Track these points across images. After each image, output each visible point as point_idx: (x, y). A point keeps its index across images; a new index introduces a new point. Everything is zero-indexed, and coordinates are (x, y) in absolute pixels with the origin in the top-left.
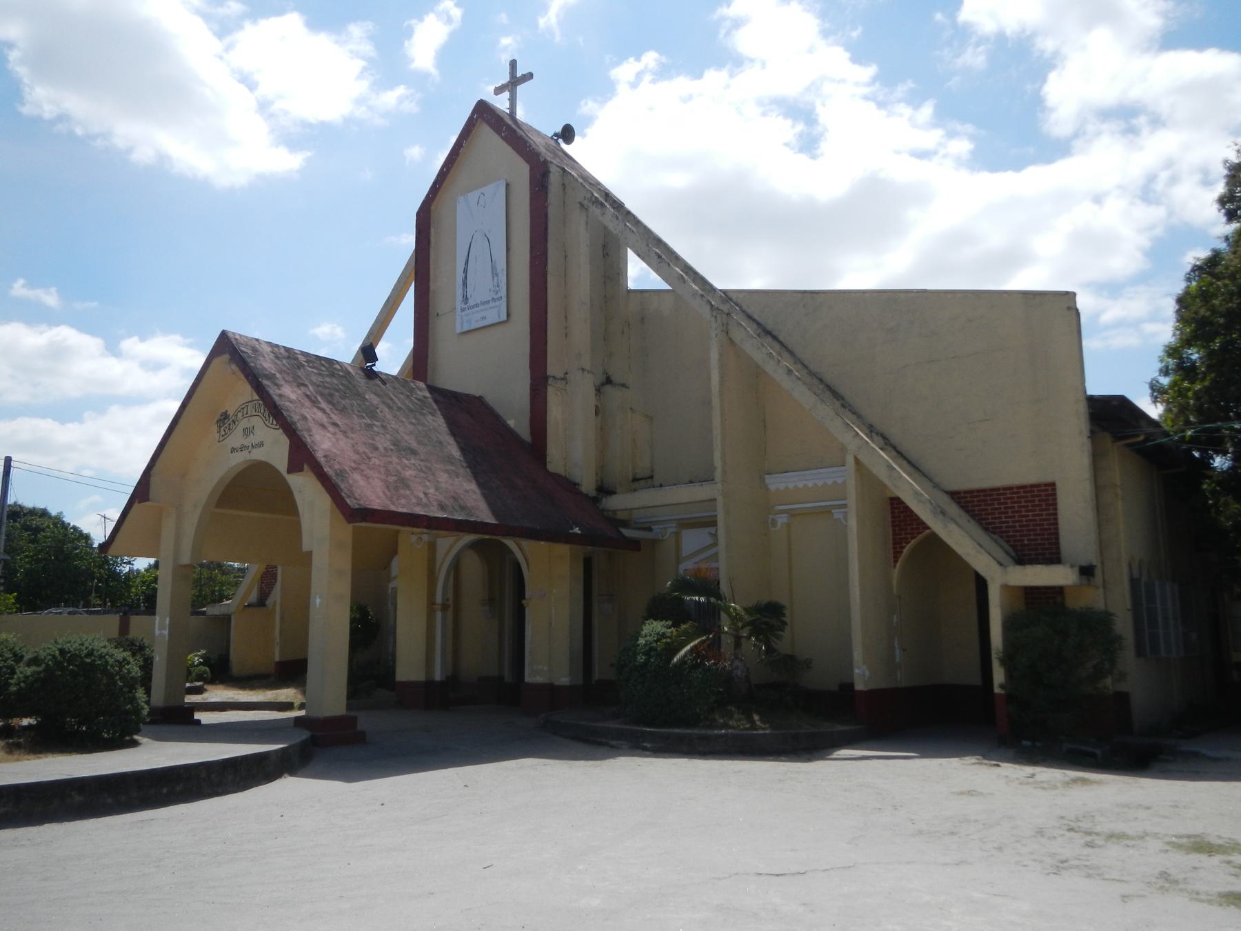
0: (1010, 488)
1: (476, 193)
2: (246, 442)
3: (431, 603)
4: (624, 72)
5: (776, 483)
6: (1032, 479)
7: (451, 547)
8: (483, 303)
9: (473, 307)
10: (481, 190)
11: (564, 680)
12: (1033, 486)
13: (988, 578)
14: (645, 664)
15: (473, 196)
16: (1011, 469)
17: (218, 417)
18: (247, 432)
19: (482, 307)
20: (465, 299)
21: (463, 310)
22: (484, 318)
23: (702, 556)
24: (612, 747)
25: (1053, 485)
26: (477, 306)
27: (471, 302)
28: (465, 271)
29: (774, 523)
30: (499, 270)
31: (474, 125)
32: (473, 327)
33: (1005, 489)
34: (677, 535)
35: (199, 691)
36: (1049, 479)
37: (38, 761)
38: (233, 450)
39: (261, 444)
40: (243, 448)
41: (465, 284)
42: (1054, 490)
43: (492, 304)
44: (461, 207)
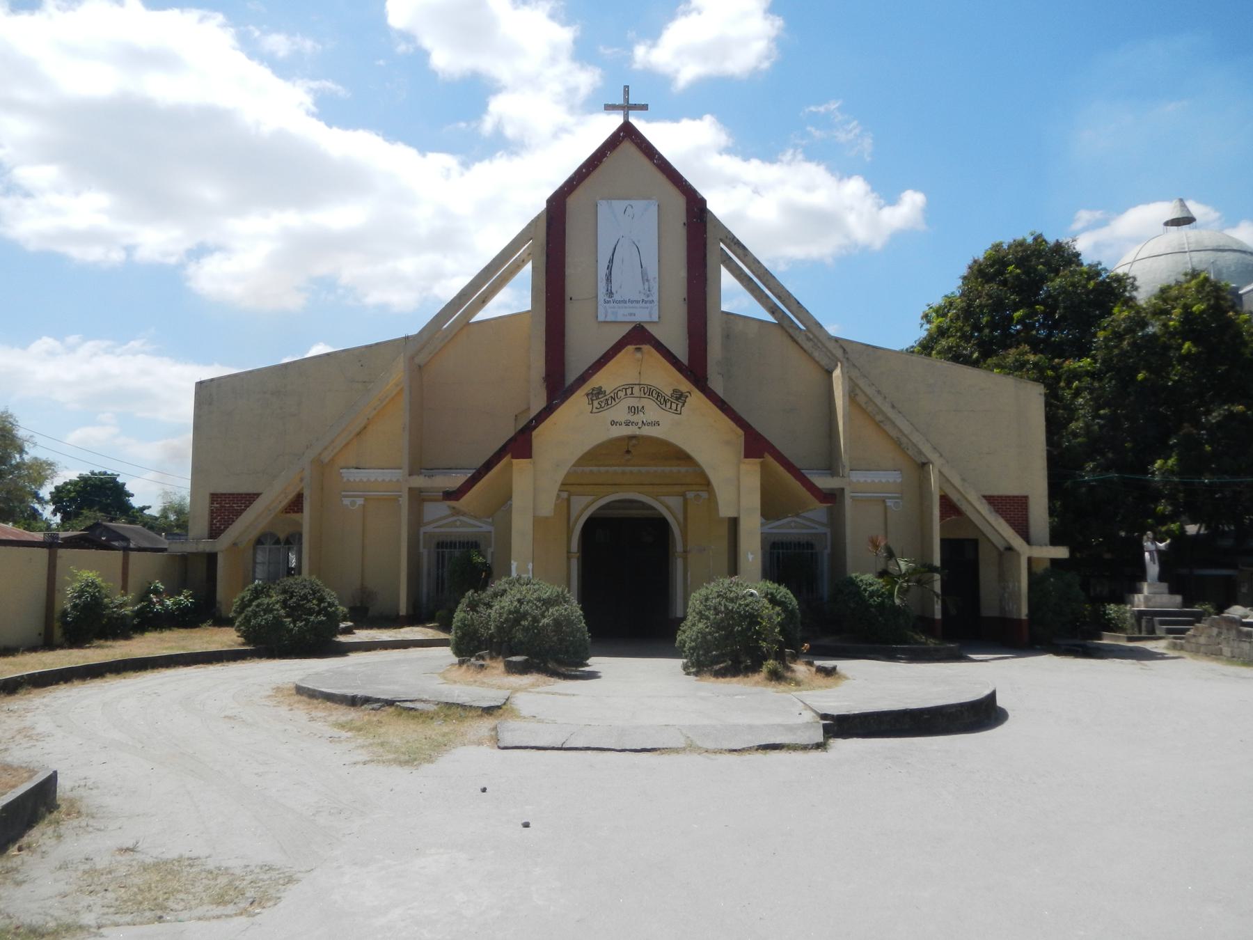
1: (627, 202)
3: (569, 552)
7: (587, 507)
10: (632, 202)
14: (883, 602)
15: (619, 205)
16: (1008, 488)
20: (610, 293)
21: (605, 302)
25: (1026, 497)
27: (617, 297)
28: (610, 268)
32: (619, 319)
35: (348, 631)
38: (613, 423)
40: (627, 424)
41: (609, 278)
43: (641, 304)
44: (603, 207)
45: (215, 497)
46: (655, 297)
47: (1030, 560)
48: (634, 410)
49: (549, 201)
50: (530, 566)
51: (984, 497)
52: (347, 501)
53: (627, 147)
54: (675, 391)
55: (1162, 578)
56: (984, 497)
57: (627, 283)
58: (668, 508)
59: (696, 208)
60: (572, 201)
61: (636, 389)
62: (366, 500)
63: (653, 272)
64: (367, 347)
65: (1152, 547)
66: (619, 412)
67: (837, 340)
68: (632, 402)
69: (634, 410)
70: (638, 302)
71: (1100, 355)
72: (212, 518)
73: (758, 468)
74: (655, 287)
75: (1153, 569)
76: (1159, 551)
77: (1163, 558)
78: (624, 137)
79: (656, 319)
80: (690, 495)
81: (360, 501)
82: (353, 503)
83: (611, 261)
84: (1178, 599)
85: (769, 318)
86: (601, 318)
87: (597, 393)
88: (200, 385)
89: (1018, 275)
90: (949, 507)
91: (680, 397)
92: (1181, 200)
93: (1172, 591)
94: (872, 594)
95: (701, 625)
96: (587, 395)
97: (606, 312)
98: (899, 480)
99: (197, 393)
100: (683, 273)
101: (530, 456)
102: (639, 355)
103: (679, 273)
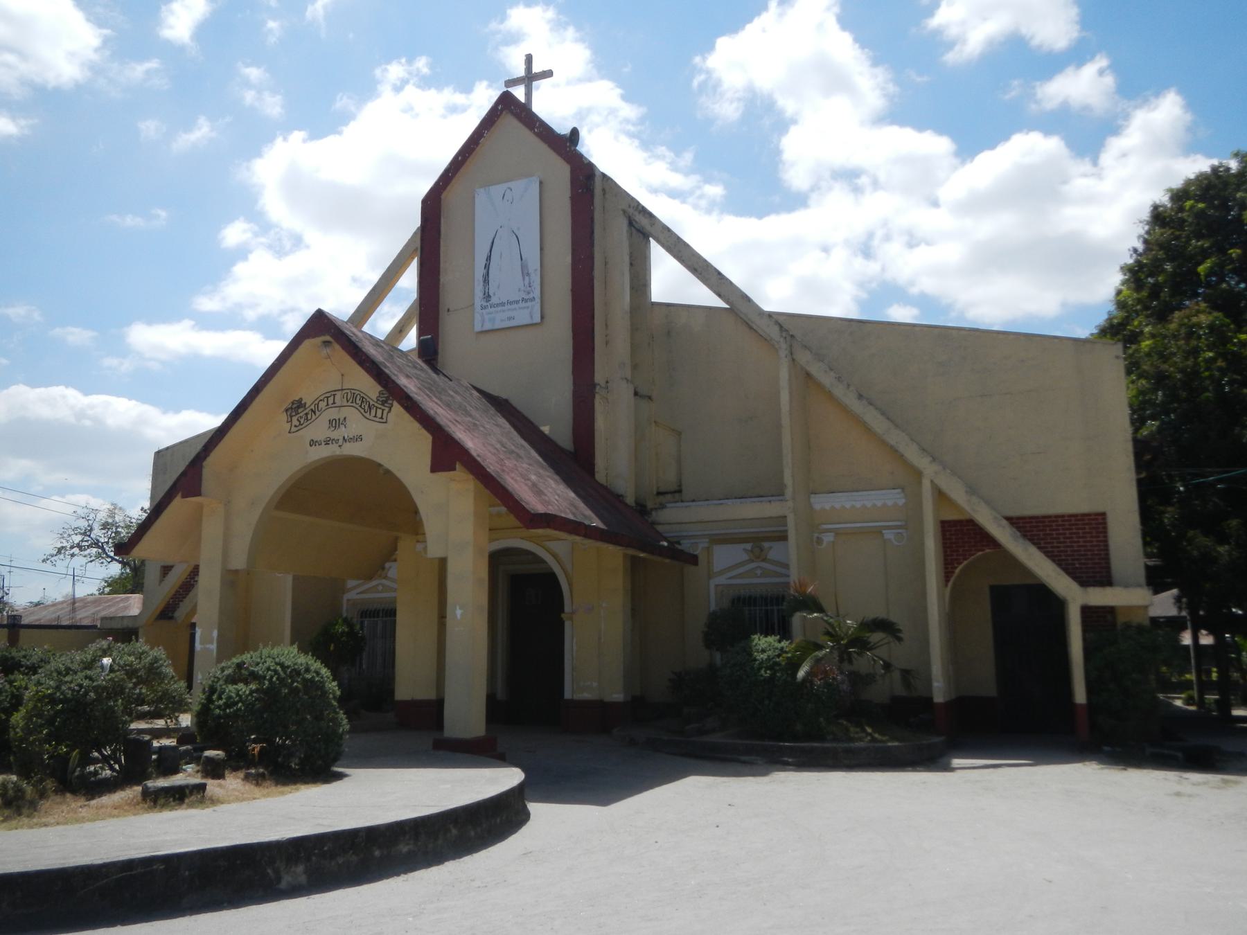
0: (1063, 516)
1: (505, 186)
2: (335, 434)
4: (396, 71)
5: (821, 503)
6: (1084, 508)
8: (510, 303)
9: (498, 305)
10: (512, 184)
11: (618, 697)
12: (1084, 515)
13: (1069, 598)
14: (772, 678)
15: (498, 190)
16: (1070, 500)
17: (287, 405)
18: (335, 424)
19: (506, 307)
20: (487, 297)
21: (483, 308)
22: (509, 319)
23: (741, 570)
24: (744, 762)
25: (1103, 515)
26: (498, 305)
27: (494, 300)
28: (487, 267)
29: (819, 541)
30: (531, 271)
31: (498, 117)
32: (496, 327)
33: (1057, 516)
34: (708, 550)
36: (1100, 509)
37: (282, 798)
39: (359, 438)
42: (1104, 519)
43: (522, 305)
44: (481, 197)
46: (537, 293)
47: (1087, 611)
48: (335, 424)
50: (215, 634)
51: (1009, 519)
56: (1009, 519)
58: (555, 556)
60: (451, 197)
61: (339, 395)
63: (534, 264)
66: (318, 428)
67: (770, 315)
68: (333, 414)
70: (517, 302)
74: (536, 279)
83: (489, 258)
85: (718, 302)
87: (296, 407)
89: (1202, 211)
90: (962, 537)
96: (287, 410)
97: (483, 319)
98: (901, 502)
100: (569, 259)
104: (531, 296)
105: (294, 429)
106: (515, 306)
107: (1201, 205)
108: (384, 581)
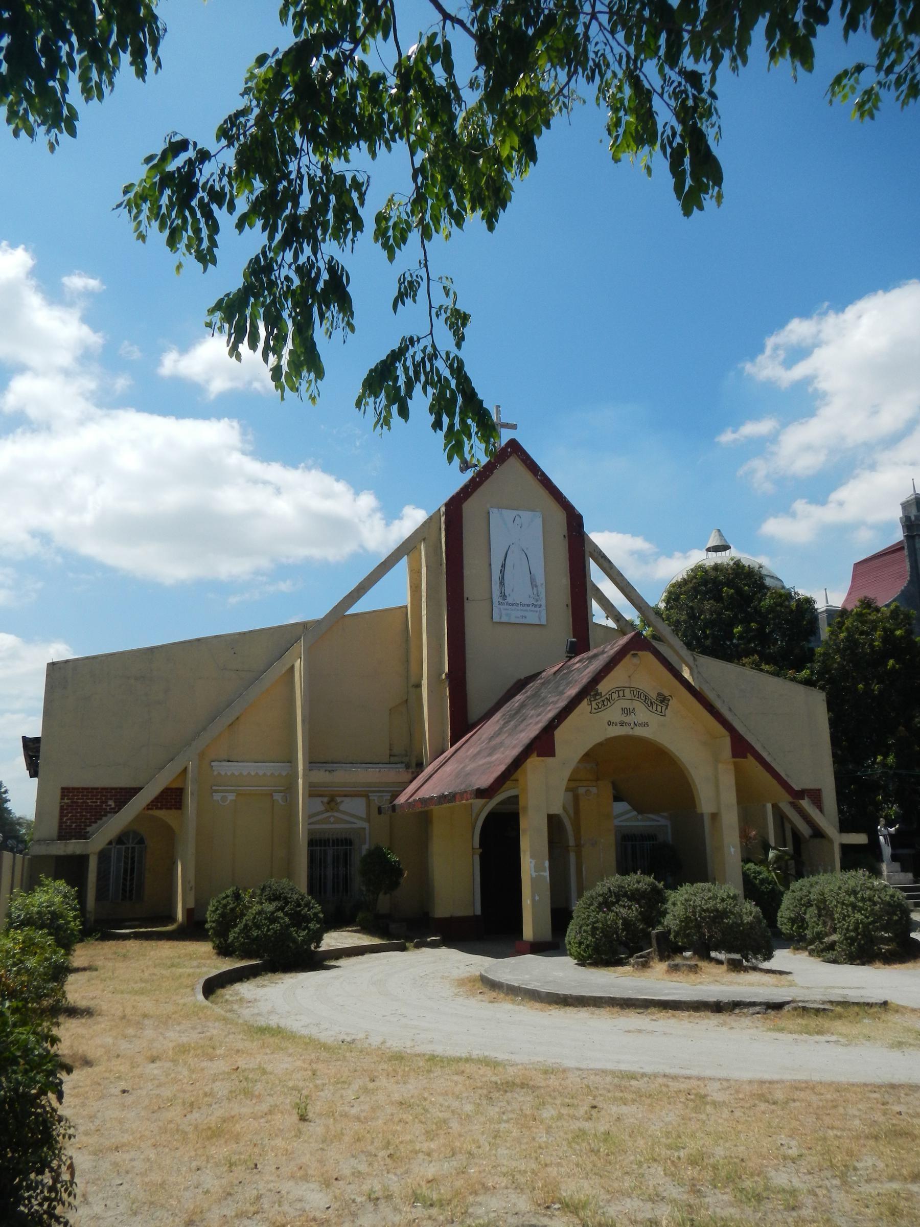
1: (515, 513)
2: (627, 719)
8: (524, 605)
9: (513, 604)
10: (520, 513)
15: (509, 514)
19: (519, 608)
22: (522, 617)
26: (513, 604)
27: (509, 600)
28: (502, 572)
30: (538, 583)
31: (508, 457)
32: (513, 620)
38: (610, 723)
39: (646, 725)
41: (502, 582)
44: (494, 515)
45: (66, 792)
46: (543, 602)
48: (626, 711)
49: (447, 505)
50: (547, 864)
52: (217, 797)
53: (513, 463)
54: (659, 694)
55: (894, 858)
57: (519, 588)
59: (574, 522)
60: (469, 508)
61: (627, 691)
62: (238, 794)
64: (240, 634)
65: (885, 832)
66: (614, 713)
68: (626, 704)
69: (626, 711)
71: (817, 666)
72: (62, 816)
73: (732, 767)
74: (542, 590)
75: (887, 851)
76: (891, 835)
77: (894, 840)
78: (511, 453)
79: (544, 622)
80: (581, 791)
81: (231, 797)
82: (224, 799)
83: (504, 566)
84: (910, 876)
86: (496, 618)
88: (53, 668)
91: (663, 700)
92: (719, 531)
93: (904, 869)
94: (763, 881)
95: (859, 916)
97: (501, 614)
99: (48, 676)
101: (554, 756)
102: (635, 661)
103: (564, 581)
104: (539, 603)
105: (594, 711)
106: (525, 608)
107: (732, 591)
108: (336, 814)
